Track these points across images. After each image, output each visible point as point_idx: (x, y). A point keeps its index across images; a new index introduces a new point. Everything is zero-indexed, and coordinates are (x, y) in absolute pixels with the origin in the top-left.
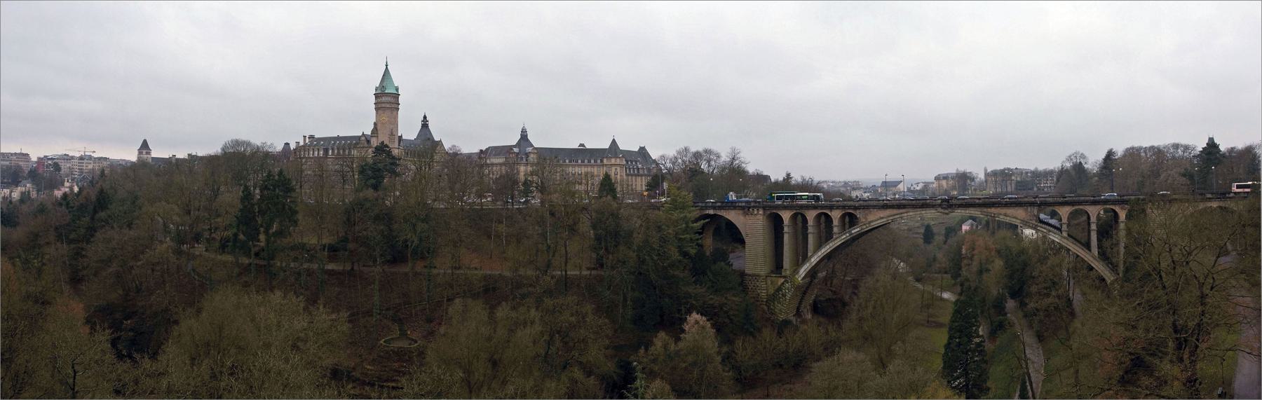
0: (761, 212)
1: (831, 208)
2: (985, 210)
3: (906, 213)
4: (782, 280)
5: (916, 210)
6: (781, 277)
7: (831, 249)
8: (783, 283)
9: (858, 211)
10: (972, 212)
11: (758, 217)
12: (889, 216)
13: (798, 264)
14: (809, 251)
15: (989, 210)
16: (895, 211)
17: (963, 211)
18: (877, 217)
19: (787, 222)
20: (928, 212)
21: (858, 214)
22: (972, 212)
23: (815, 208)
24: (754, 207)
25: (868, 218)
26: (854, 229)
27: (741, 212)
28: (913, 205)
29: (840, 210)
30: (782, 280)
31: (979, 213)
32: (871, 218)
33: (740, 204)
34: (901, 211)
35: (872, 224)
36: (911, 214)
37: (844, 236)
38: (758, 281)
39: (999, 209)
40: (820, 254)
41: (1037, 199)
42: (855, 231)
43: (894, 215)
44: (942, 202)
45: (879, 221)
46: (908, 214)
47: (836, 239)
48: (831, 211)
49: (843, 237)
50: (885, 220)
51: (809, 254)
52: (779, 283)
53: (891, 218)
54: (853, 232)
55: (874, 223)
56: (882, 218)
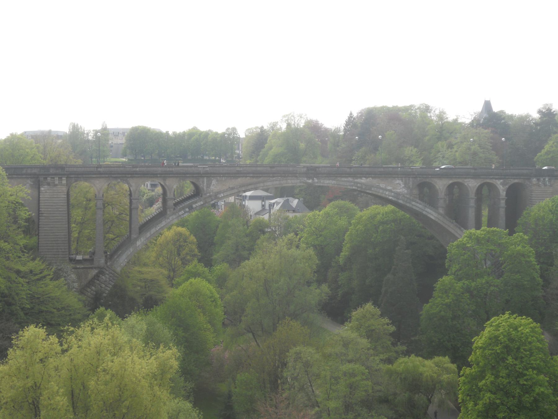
6: (92, 268)
15: (359, 180)
16: (248, 180)
21: (203, 183)
26: (196, 203)
27: (30, 182)
30: (94, 272)
34: (255, 180)
52: (90, 276)
56: (233, 188)
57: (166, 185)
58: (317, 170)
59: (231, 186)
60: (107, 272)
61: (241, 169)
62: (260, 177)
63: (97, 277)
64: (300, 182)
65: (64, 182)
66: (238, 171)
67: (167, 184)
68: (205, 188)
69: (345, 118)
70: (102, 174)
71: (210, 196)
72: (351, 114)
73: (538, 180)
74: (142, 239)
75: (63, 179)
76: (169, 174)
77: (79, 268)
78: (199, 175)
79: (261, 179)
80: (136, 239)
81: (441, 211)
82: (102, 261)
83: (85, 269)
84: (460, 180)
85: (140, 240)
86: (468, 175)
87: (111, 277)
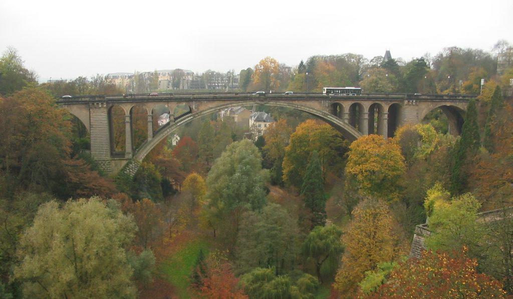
2: (291, 102)
3: (231, 104)
10: (282, 104)
13: (136, 147)
15: (294, 102)
16: (222, 103)
18: (206, 108)
20: (249, 103)
22: (282, 104)
24: (99, 101)
27: (83, 106)
29: (176, 102)
30: (124, 163)
31: (286, 104)
32: (202, 108)
33: (83, 99)
34: (226, 103)
35: (203, 113)
38: (104, 165)
39: (301, 101)
44: (260, 96)
45: (208, 111)
47: (173, 125)
50: (213, 109)
51: (150, 139)
53: (218, 108)
56: (211, 108)
63: (127, 165)
65: (105, 106)
68: (194, 108)
69: (298, 63)
70: (128, 100)
71: (197, 113)
72: (302, 62)
73: (409, 102)
78: (188, 100)
81: (346, 121)
82: (131, 156)
84: (359, 102)
86: (363, 99)
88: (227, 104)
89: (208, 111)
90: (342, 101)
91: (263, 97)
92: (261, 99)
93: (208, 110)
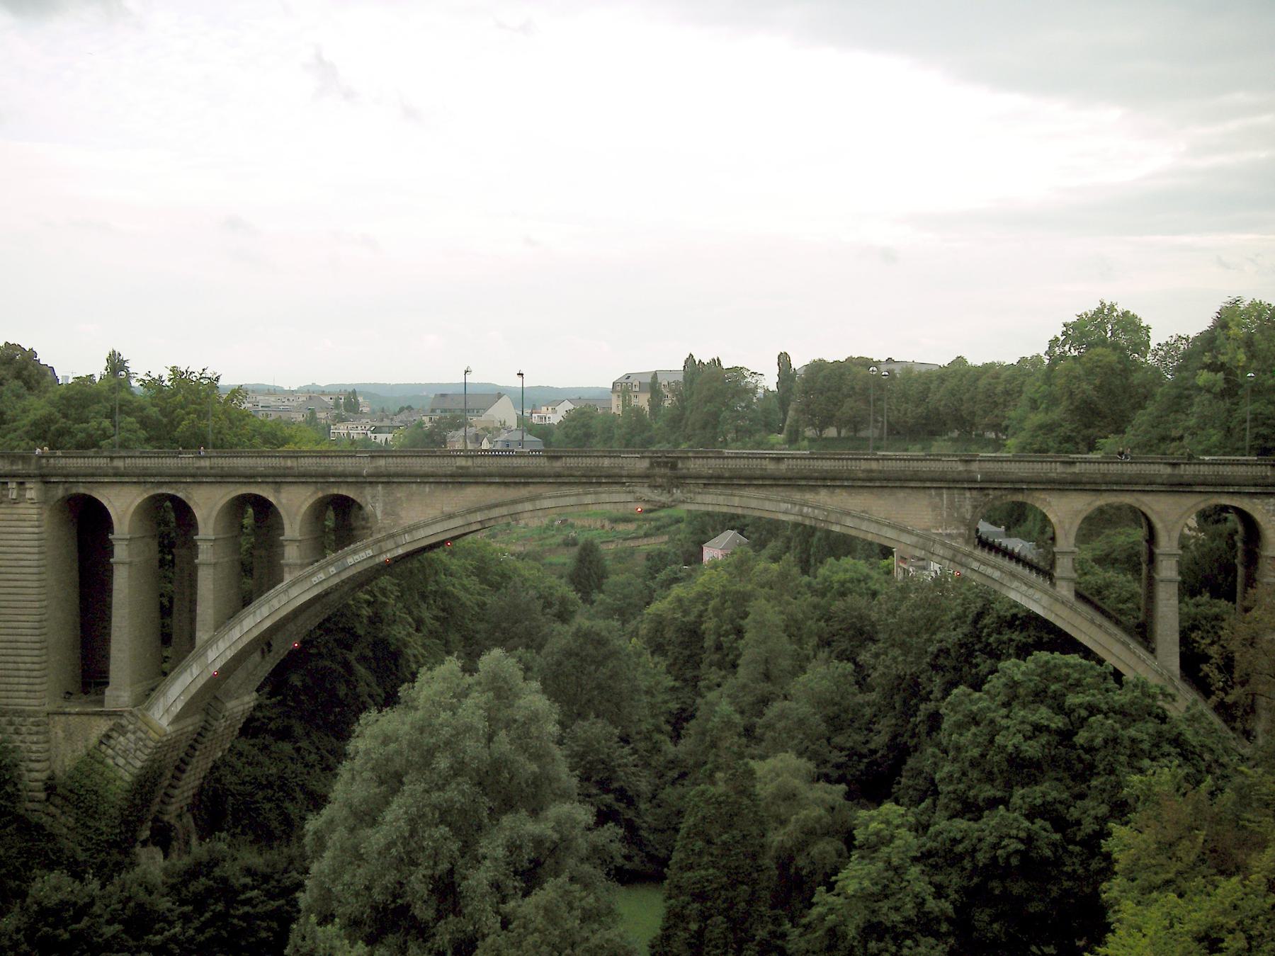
0: (32, 492)
1: (279, 479)
2: (797, 496)
3: (531, 499)
4: (103, 726)
5: (565, 490)
7: (276, 618)
8: (108, 737)
9: (368, 491)
11: (22, 509)
12: (471, 511)
14: (199, 625)
15: (809, 496)
17: (721, 499)
18: (432, 513)
19: (125, 528)
20: (604, 497)
21: (373, 502)
22: (754, 504)
23: (222, 478)
25: (403, 514)
26: (355, 552)
28: (558, 476)
29: (312, 488)
30: (103, 726)
34: (512, 493)
35: (421, 533)
36: (547, 503)
37: (322, 576)
38: (17, 732)
40: (236, 633)
41: (975, 466)
42: (358, 558)
43: (490, 507)
44: (652, 464)
46: (539, 504)
47: (294, 584)
48: (277, 491)
49: (315, 580)
50: (458, 522)
51: (201, 636)
53: (479, 517)
54: (350, 561)
55: (429, 531)
56: (450, 516)
57: (281, 503)
58: (680, 465)
59: (447, 509)
60: (131, 727)
61: (469, 463)
62: (526, 484)
64: (638, 500)
66: (461, 468)
67: (284, 501)
71: (392, 536)
74: (220, 643)
75: (28, 486)
76: (285, 476)
77: (69, 714)
79: (524, 492)
80: (209, 643)
81: (1065, 591)
83: (83, 717)
85: (215, 646)
87: (141, 739)
88: (514, 502)
89: (438, 528)
90: (1043, 495)
91: (663, 471)
92: (659, 480)
93: (435, 521)
